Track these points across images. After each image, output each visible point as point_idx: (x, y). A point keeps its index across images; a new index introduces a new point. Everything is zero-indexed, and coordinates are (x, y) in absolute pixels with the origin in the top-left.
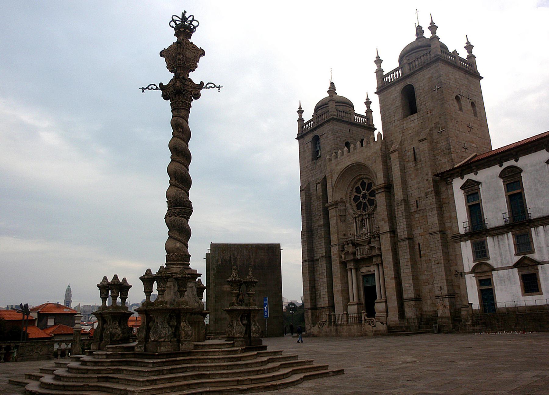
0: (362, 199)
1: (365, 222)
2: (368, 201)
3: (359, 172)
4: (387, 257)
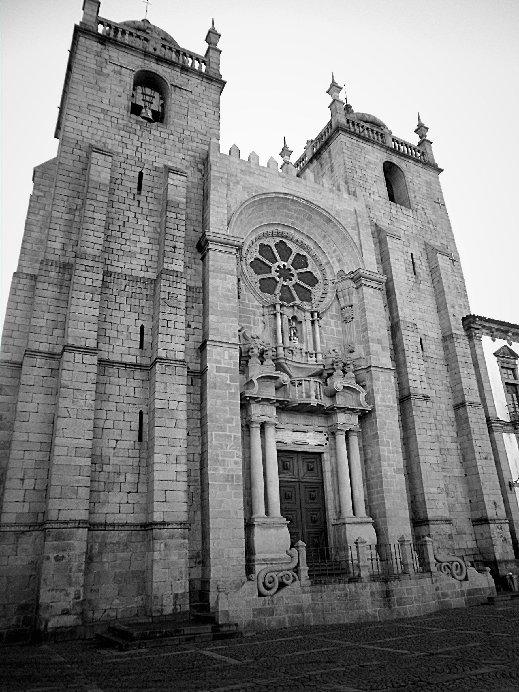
0: (279, 277)
1: (307, 327)
2: (293, 286)
3: (291, 220)
4: (388, 421)
